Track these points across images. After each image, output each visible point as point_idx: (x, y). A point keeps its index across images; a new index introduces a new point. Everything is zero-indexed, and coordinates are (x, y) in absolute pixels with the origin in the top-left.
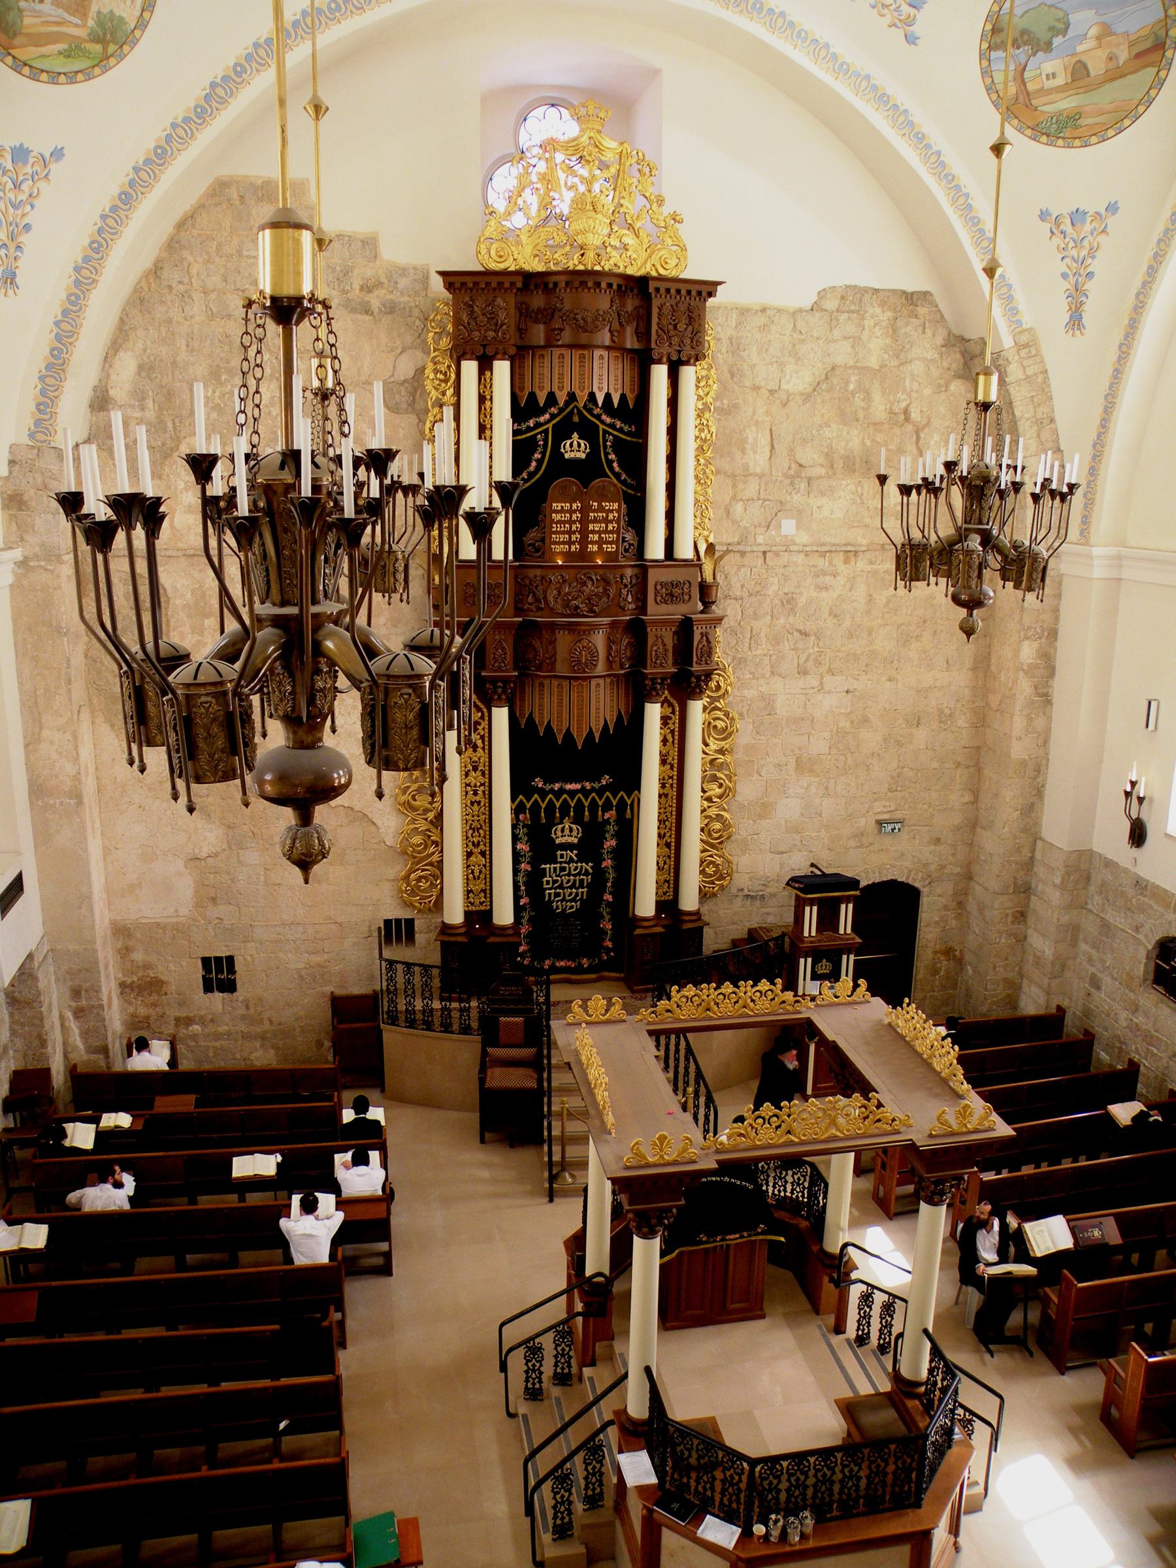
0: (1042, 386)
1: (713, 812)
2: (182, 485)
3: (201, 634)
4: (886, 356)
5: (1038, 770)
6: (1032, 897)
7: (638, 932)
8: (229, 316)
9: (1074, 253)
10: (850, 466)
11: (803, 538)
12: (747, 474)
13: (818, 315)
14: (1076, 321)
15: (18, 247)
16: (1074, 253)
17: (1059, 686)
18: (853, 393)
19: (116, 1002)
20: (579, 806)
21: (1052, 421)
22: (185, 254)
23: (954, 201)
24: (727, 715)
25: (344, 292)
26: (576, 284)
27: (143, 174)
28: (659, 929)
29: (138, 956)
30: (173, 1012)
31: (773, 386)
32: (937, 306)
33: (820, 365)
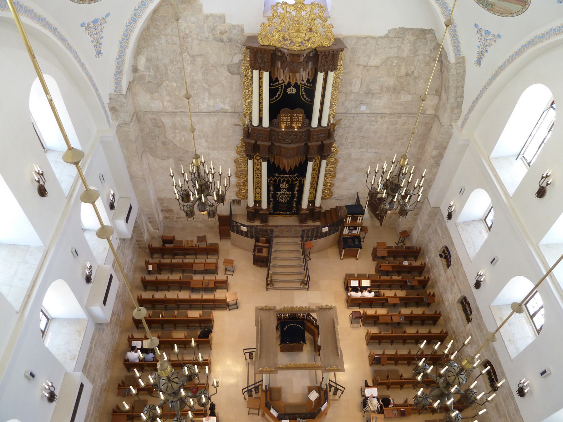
0: (462, 76)
1: (328, 181)
3: (176, 134)
5: (431, 182)
6: (421, 212)
7: (301, 212)
8: (175, 44)
10: (388, 90)
11: (368, 111)
12: (351, 93)
13: (386, 39)
14: (479, 62)
15: (100, 44)
16: (484, 42)
17: (443, 162)
18: (394, 67)
19: (160, 214)
20: (288, 180)
21: (463, 87)
22: (157, 23)
27: (138, 11)
28: (308, 212)
29: (165, 205)
30: (176, 216)
31: (364, 64)
33: (384, 56)
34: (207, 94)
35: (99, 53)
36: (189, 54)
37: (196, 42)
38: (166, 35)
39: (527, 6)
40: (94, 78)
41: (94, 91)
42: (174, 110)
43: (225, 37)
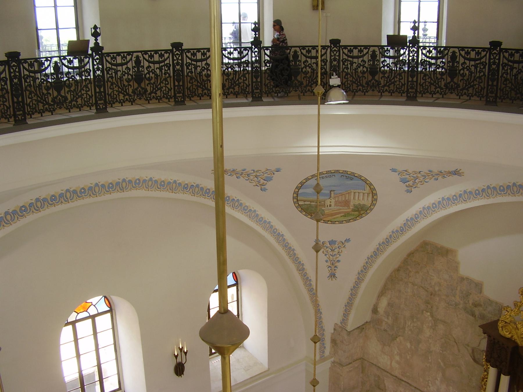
2: (396, 353)
15: (336, 267)
34: (441, 374)
35: (333, 276)
36: (432, 316)
38: (413, 284)
41: (312, 311)
42: (400, 376)
43: (477, 311)
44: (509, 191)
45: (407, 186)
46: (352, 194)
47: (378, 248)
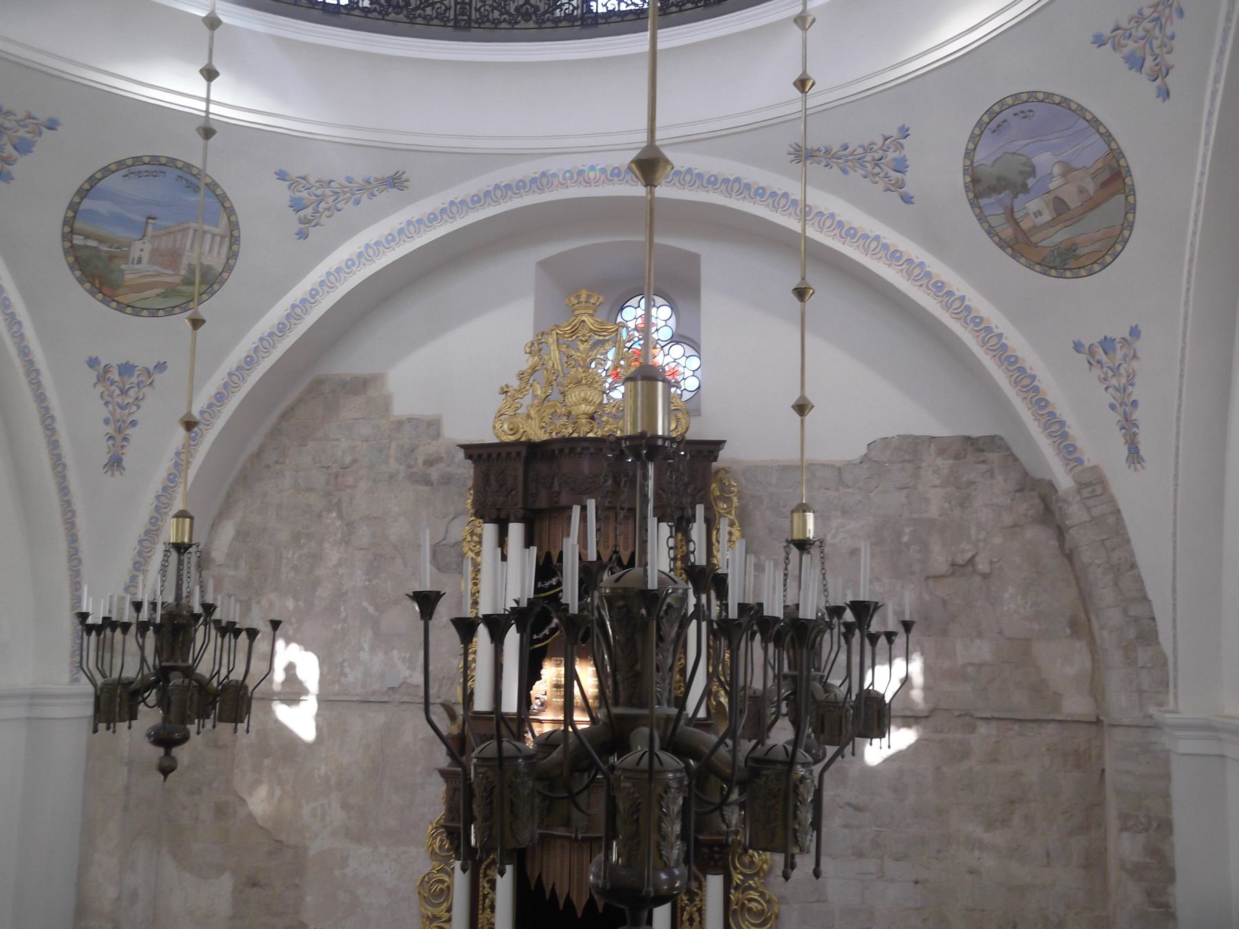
0: (1114, 529)
4: (946, 505)
9: (1114, 382)
14: (1134, 455)
15: (125, 439)
16: (1114, 382)
21: (1133, 566)
23: (984, 343)
24: (762, 895)
25: (410, 467)
26: (567, 451)
32: (1008, 449)
34: (369, 633)
35: (115, 463)
36: (340, 516)
37: (363, 485)
39: (1128, 180)
40: (81, 522)
41: (62, 545)
43: (434, 473)
44: (489, 200)
45: (301, 222)
46: (191, 232)
47: (226, 383)
